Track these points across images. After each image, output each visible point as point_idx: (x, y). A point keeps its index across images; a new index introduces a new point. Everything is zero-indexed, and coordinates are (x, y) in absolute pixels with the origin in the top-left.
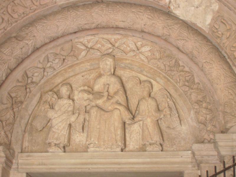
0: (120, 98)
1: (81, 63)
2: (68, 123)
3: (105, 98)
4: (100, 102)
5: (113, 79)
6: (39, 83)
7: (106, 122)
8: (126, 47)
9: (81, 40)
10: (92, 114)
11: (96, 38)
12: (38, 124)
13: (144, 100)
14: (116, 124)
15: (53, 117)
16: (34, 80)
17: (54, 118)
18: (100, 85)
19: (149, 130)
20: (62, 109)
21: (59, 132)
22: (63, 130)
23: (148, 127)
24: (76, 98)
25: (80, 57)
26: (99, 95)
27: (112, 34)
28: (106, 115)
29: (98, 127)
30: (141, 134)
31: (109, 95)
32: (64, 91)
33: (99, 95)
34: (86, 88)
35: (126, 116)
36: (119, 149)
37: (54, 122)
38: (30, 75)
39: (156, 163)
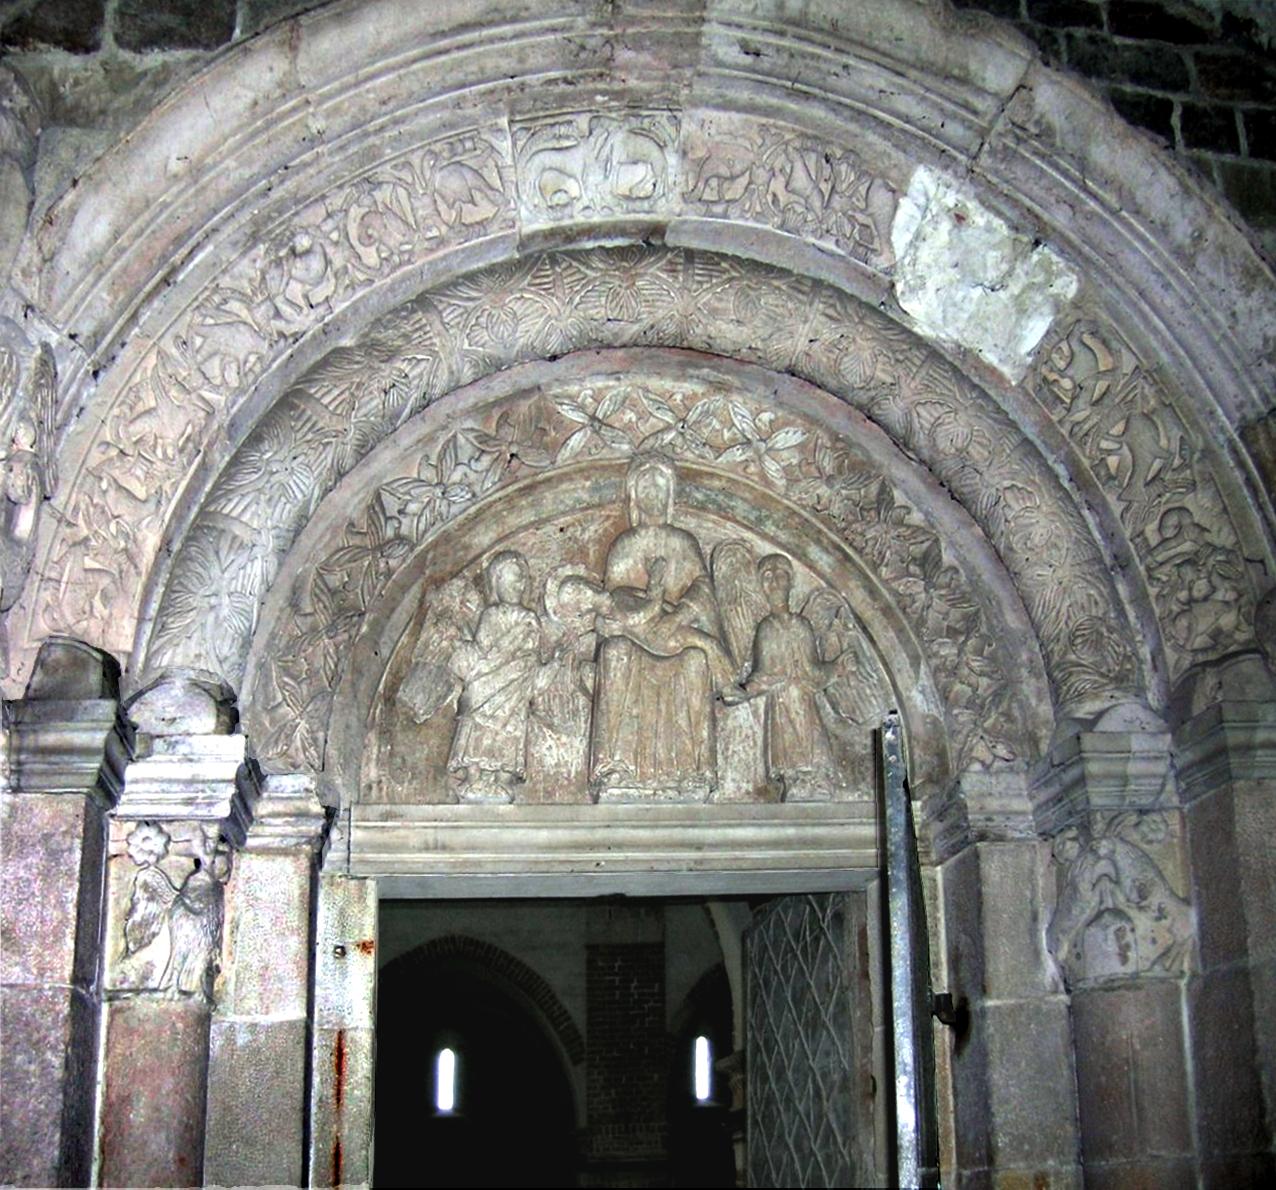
1: (565, 477)
6: (419, 543)
7: (658, 695)
8: (718, 427)
9: (574, 389)
10: (613, 664)
11: (622, 387)
12: (416, 697)
13: (777, 624)
14: (696, 702)
15: (474, 673)
16: (404, 530)
17: (479, 675)
18: (631, 562)
19: (794, 728)
20: (505, 643)
21: (498, 727)
22: (513, 722)
23: (793, 715)
25: (565, 454)
26: (629, 597)
27: (677, 379)
29: (635, 712)
30: (760, 742)
34: (581, 570)
37: (478, 692)
38: (392, 505)
39: (816, 843)
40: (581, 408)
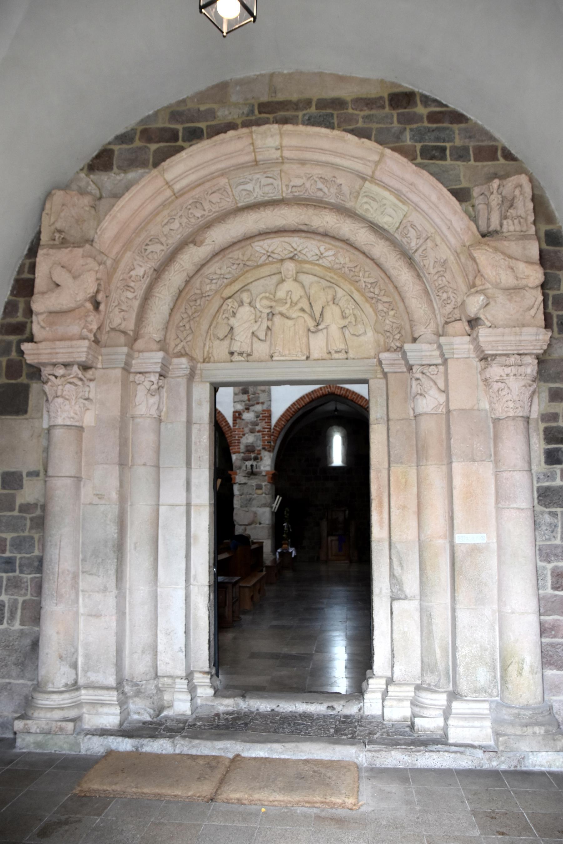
0: (304, 304)
2: (251, 331)
3: (288, 305)
4: (283, 309)
5: (296, 284)
24: (258, 306)
26: (283, 302)
28: (290, 323)
31: (291, 302)
32: (245, 297)
33: (283, 302)
34: (267, 295)
35: (311, 324)
36: (304, 358)
40: (264, 249)
